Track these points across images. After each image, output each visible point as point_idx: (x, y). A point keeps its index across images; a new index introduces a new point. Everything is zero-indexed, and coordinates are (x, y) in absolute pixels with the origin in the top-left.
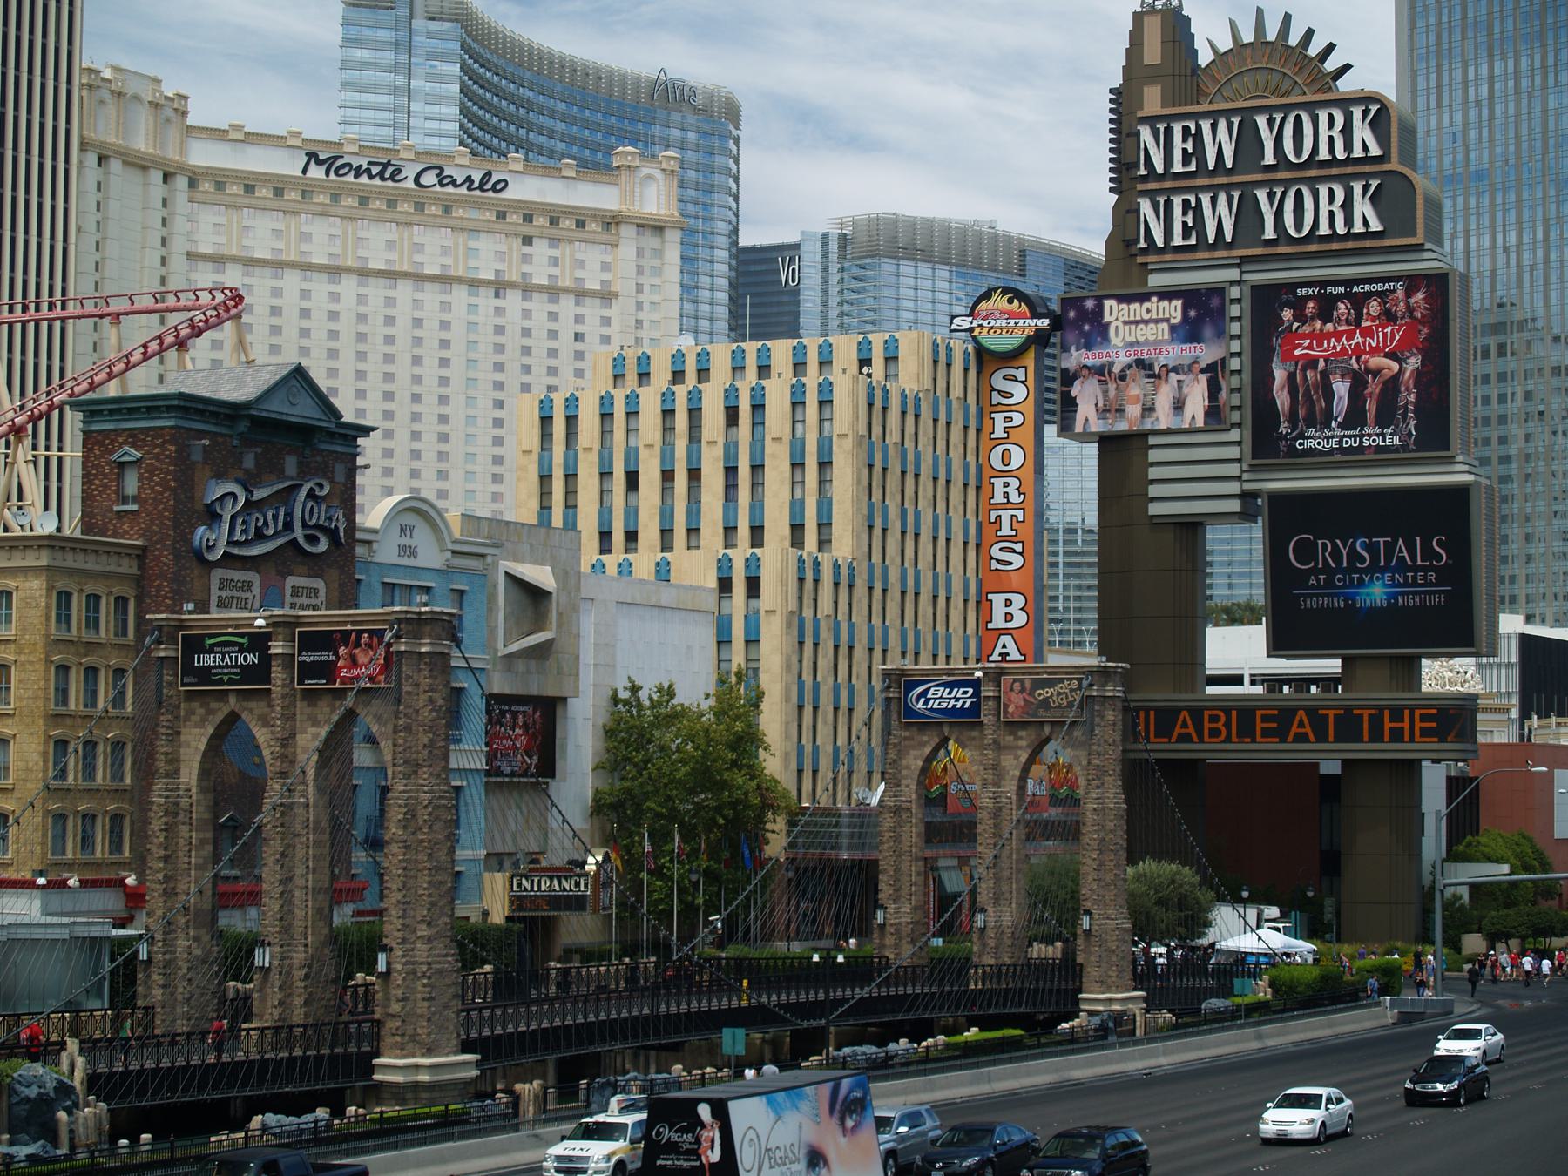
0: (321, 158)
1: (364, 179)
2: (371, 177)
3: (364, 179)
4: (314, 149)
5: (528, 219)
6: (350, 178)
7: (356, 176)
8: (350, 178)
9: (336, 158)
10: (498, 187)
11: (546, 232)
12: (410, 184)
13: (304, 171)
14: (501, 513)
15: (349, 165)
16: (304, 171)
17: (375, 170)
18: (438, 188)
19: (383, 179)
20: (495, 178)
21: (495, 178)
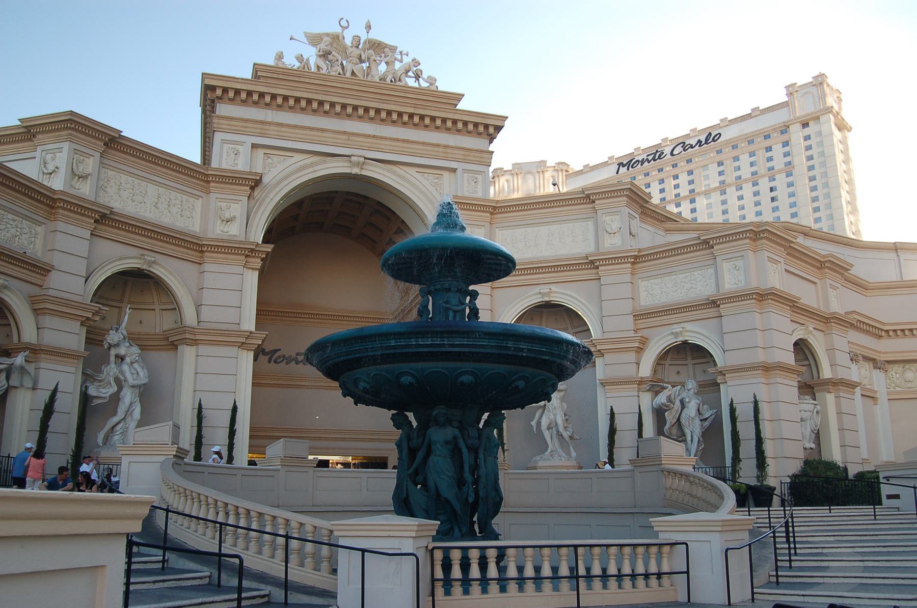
0: (624, 163)
4: (621, 161)
7: (641, 165)
9: (631, 161)
10: (716, 138)
12: (669, 156)
13: (617, 173)
15: (638, 161)
16: (617, 173)
18: (683, 152)
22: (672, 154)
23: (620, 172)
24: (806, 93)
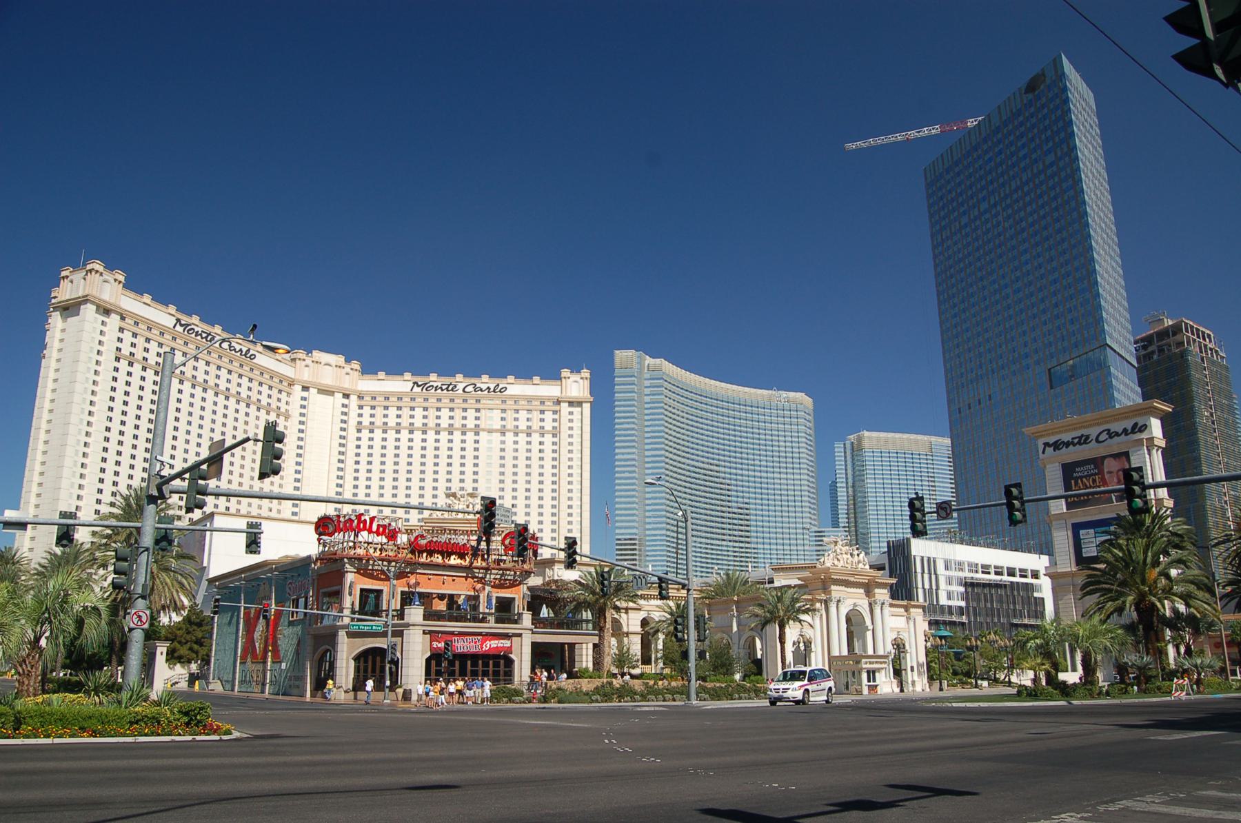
1: (439, 391)
2: (442, 390)
3: (439, 391)
7: (436, 390)
8: (433, 391)
9: (426, 384)
17: (444, 387)
18: (473, 392)
19: (448, 391)
20: (501, 386)
21: (501, 386)
22: (464, 391)
23: (414, 390)
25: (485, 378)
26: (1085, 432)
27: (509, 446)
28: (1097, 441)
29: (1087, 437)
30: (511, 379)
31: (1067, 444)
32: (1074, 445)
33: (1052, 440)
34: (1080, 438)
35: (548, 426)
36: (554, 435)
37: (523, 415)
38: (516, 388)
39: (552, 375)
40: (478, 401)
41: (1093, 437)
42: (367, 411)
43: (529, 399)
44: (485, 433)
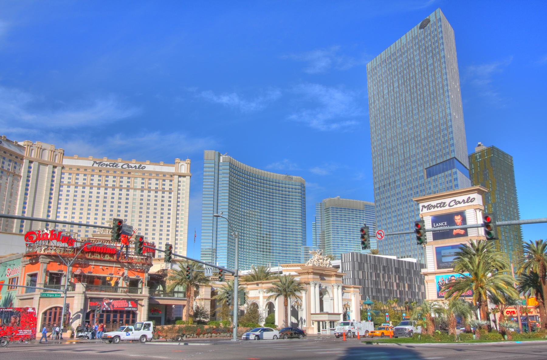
1: (108, 167)
2: (110, 166)
3: (108, 167)
5: (86, 170)
6: (105, 166)
8: (105, 166)
9: (101, 163)
11: (127, 175)
12: (120, 168)
13: (93, 165)
14: (89, 222)
15: (104, 164)
17: (111, 165)
19: (113, 167)
20: (143, 165)
21: (143, 165)
22: (122, 167)
24: (182, 165)
25: (134, 161)
26: (443, 201)
27: (145, 197)
28: (449, 206)
29: (444, 203)
30: (148, 162)
31: (434, 207)
32: (438, 207)
33: (426, 204)
34: (440, 204)
35: (167, 188)
36: (170, 193)
37: (153, 181)
38: (150, 167)
39: (170, 161)
40: (129, 173)
41: (447, 203)
42: (66, 176)
43: (157, 173)
44: (133, 190)
